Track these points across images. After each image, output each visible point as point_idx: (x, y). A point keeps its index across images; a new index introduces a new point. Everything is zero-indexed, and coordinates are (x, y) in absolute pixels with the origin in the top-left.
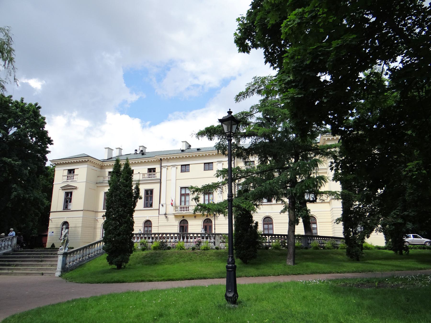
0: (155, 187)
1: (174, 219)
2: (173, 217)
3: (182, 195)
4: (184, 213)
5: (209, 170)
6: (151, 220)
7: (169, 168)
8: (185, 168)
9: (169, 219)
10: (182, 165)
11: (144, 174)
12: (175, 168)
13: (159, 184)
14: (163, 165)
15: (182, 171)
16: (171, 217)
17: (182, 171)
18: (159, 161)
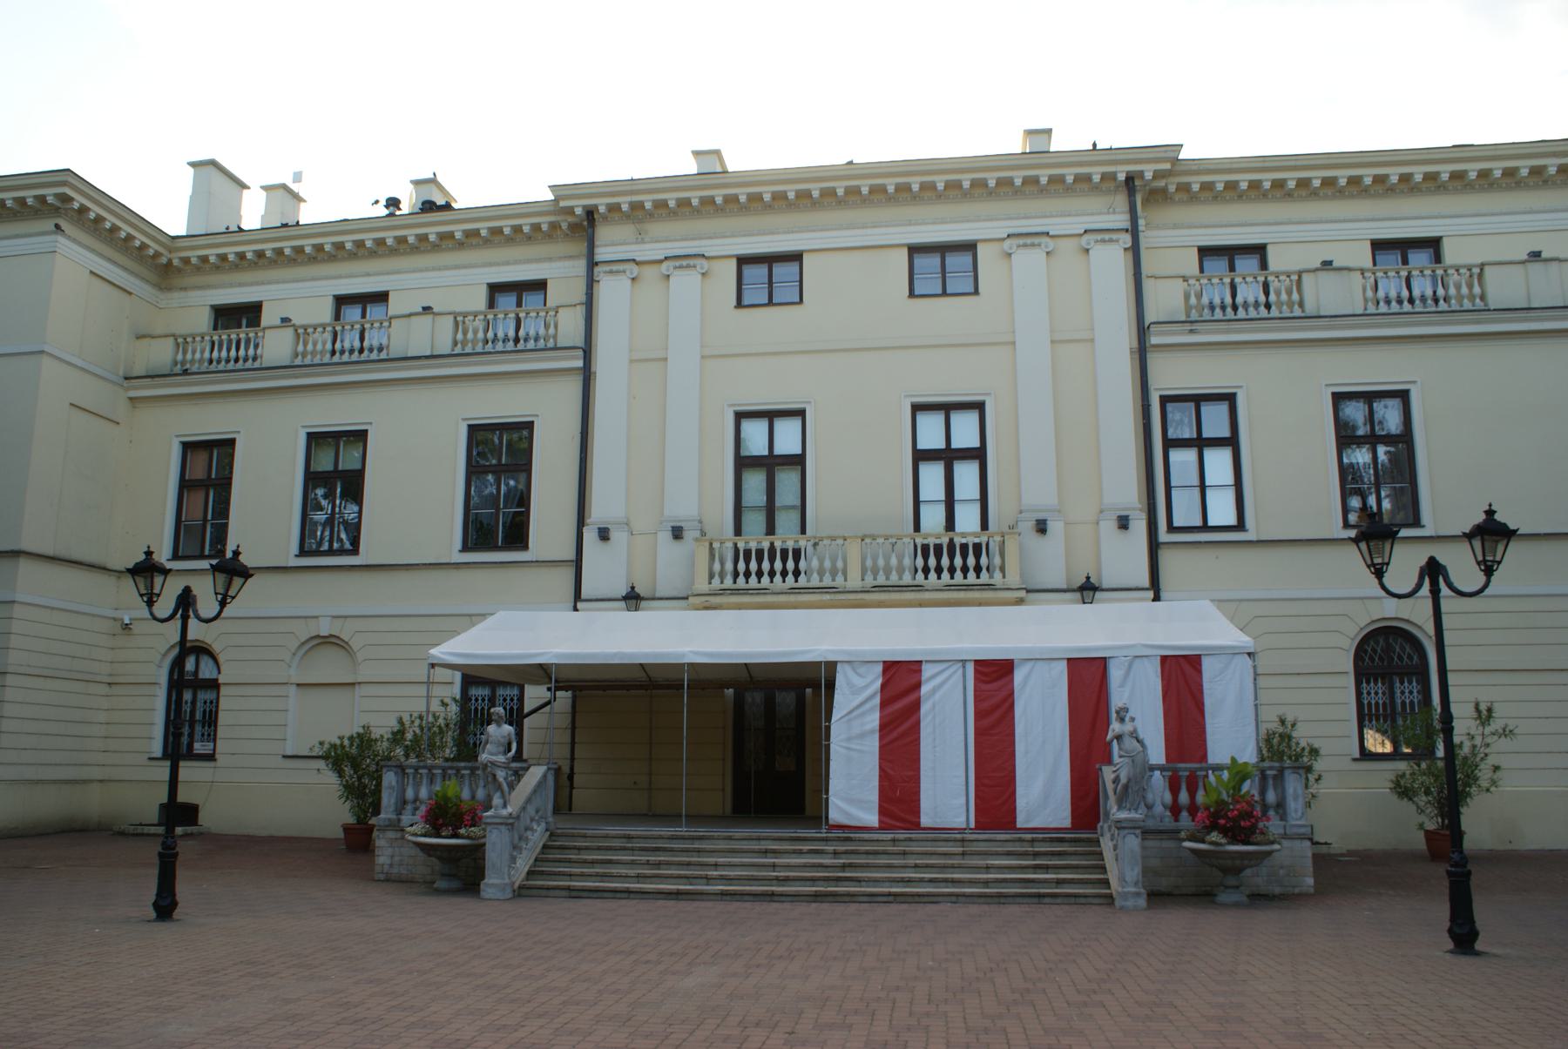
0: (549, 410)
8: (768, 276)
11: (459, 320)
14: (602, 254)
18: (574, 227)
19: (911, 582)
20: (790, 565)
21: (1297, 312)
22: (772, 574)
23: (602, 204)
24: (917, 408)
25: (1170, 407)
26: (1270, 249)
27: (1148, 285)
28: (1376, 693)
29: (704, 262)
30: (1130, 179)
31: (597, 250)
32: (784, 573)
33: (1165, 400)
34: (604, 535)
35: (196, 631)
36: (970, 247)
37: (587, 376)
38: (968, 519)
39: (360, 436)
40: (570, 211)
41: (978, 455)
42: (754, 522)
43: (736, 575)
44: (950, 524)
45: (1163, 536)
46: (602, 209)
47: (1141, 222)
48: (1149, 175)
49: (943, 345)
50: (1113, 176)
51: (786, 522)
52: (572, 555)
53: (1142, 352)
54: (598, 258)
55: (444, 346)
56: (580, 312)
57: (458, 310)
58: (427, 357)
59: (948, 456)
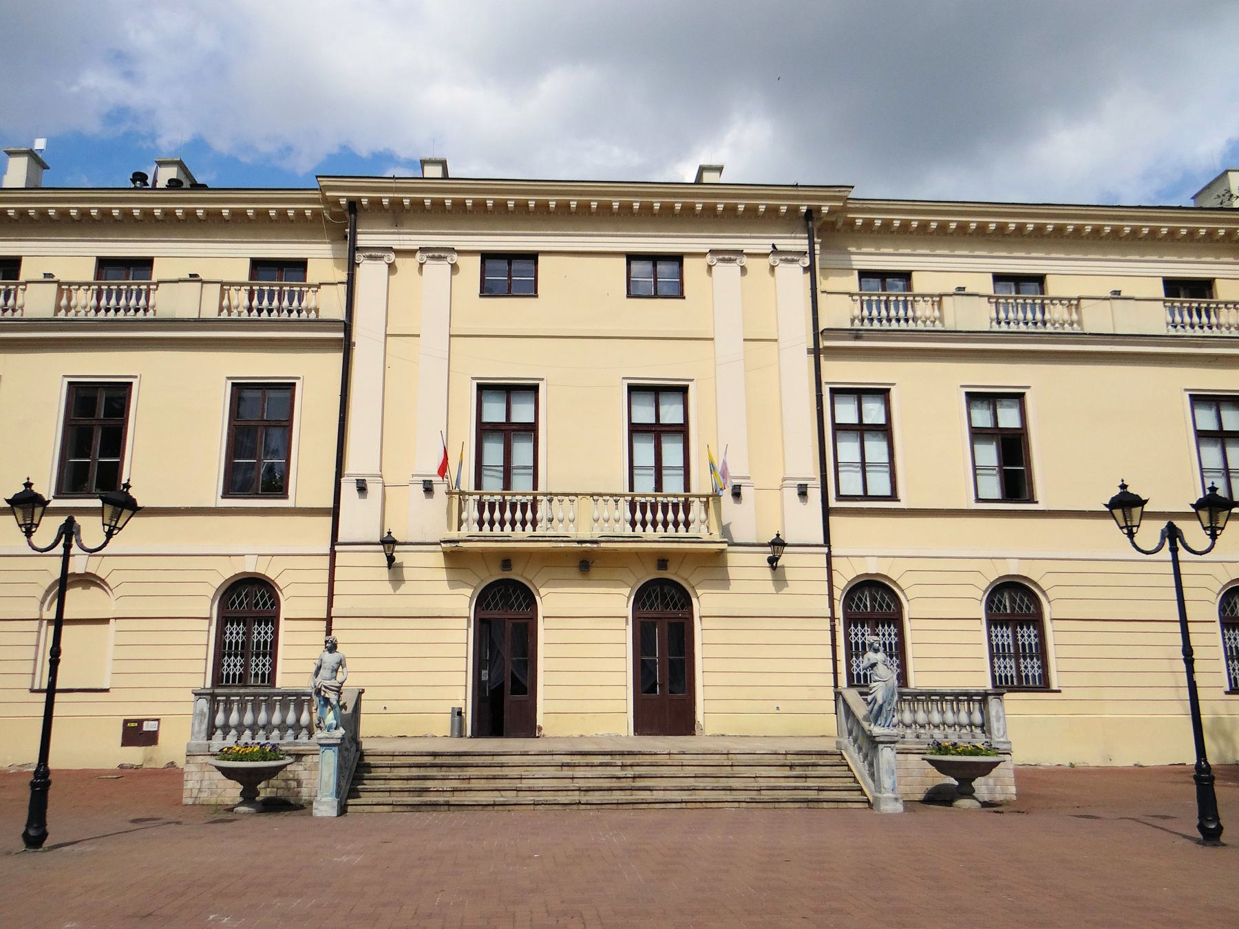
0: (313, 375)
1: (443, 574)
2: (439, 560)
3: (484, 430)
4: (518, 537)
5: (656, 296)
6: (271, 574)
7: (400, 262)
9: (407, 574)
10: (486, 256)
12: (444, 267)
13: (339, 357)
14: (363, 240)
15: (487, 290)
16: (426, 568)
17: (487, 290)
19: (632, 534)
20: (529, 515)
21: (938, 326)
22: (513, 523)
23: (365, 198)
24: (633, 389)
25: (837, 398)
26: (1049, 279)
27: (821, 298)
28: (1005, 636)
29: (455, 256)
30: (809, 211)
31: (359, 237)
32: (524, 523)
33: (834, 392)
34: (362, 488)
35: (79, 564)
36: (678, 258)
37: (347, 346)
38: (673, 484)
39: (532, 389)
40: (335, 201)
41: (682, 430)
42: (493, 484)
43: (481, 523)
44: (659, 486)
45: (833, 503)
46: (365, 201)
47: (817, 247)
48: (825, 210)
49: (653, 338)
50: (797, 209)
51: (522, 483)
52: (330, 504)
53: (816, 352)
54: (360, 243)
55: (211, 312)
56: (343, 289)
57: (225, 280)
58: (195, 320)
59: (861, 430)
